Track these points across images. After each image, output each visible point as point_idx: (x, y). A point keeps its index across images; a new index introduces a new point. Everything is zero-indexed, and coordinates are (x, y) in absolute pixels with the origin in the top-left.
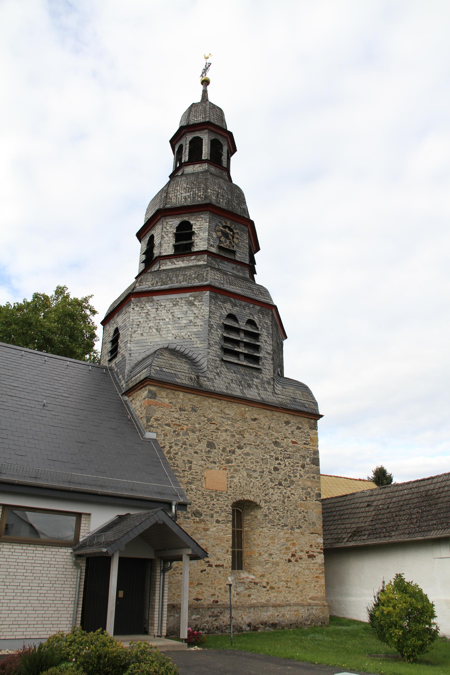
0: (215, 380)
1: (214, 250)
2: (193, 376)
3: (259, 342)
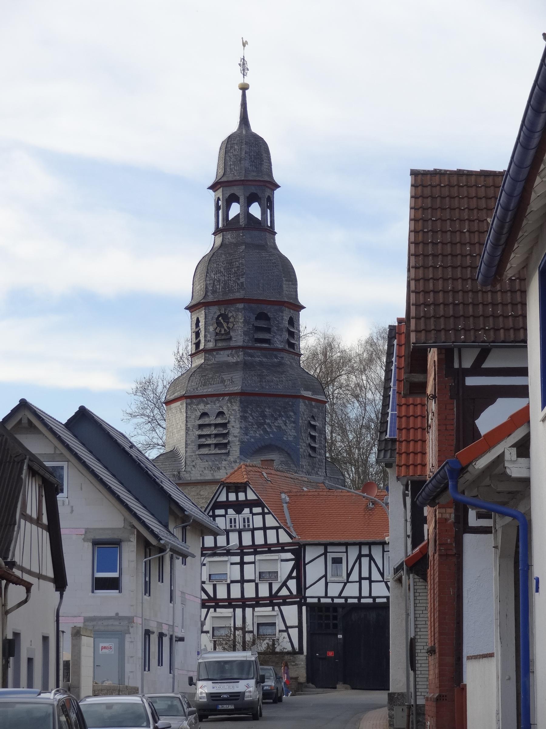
0: (192, 472)
1: (211, 345)
2: (175, 473)
3: (227, 429)
